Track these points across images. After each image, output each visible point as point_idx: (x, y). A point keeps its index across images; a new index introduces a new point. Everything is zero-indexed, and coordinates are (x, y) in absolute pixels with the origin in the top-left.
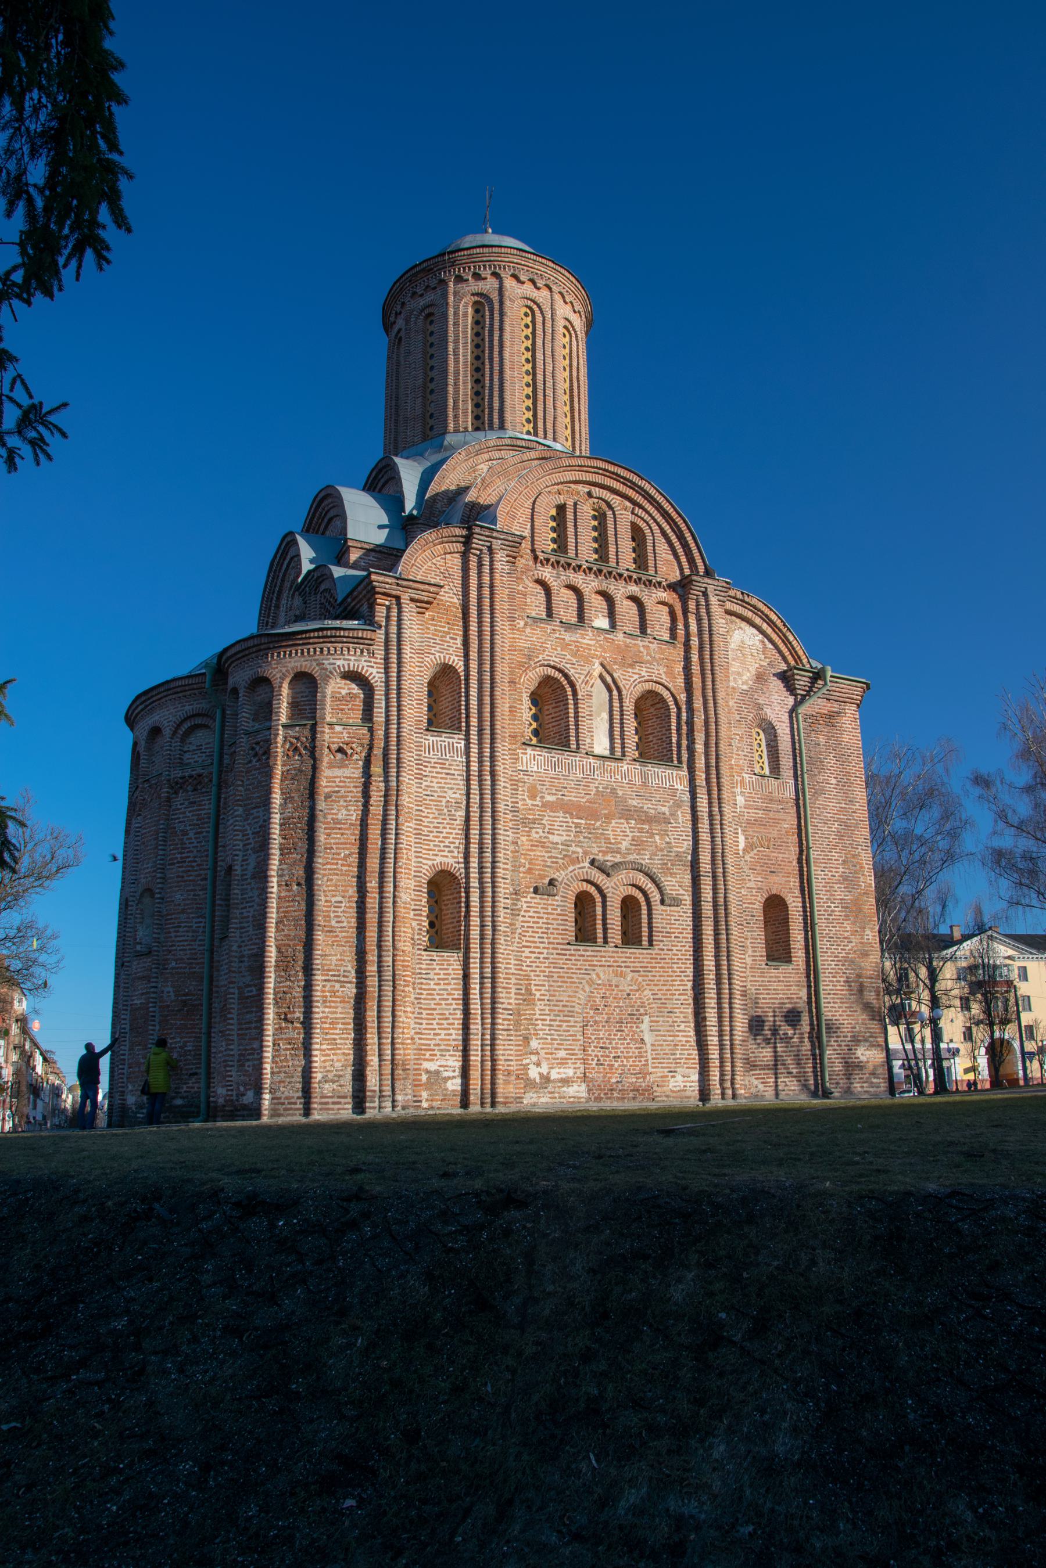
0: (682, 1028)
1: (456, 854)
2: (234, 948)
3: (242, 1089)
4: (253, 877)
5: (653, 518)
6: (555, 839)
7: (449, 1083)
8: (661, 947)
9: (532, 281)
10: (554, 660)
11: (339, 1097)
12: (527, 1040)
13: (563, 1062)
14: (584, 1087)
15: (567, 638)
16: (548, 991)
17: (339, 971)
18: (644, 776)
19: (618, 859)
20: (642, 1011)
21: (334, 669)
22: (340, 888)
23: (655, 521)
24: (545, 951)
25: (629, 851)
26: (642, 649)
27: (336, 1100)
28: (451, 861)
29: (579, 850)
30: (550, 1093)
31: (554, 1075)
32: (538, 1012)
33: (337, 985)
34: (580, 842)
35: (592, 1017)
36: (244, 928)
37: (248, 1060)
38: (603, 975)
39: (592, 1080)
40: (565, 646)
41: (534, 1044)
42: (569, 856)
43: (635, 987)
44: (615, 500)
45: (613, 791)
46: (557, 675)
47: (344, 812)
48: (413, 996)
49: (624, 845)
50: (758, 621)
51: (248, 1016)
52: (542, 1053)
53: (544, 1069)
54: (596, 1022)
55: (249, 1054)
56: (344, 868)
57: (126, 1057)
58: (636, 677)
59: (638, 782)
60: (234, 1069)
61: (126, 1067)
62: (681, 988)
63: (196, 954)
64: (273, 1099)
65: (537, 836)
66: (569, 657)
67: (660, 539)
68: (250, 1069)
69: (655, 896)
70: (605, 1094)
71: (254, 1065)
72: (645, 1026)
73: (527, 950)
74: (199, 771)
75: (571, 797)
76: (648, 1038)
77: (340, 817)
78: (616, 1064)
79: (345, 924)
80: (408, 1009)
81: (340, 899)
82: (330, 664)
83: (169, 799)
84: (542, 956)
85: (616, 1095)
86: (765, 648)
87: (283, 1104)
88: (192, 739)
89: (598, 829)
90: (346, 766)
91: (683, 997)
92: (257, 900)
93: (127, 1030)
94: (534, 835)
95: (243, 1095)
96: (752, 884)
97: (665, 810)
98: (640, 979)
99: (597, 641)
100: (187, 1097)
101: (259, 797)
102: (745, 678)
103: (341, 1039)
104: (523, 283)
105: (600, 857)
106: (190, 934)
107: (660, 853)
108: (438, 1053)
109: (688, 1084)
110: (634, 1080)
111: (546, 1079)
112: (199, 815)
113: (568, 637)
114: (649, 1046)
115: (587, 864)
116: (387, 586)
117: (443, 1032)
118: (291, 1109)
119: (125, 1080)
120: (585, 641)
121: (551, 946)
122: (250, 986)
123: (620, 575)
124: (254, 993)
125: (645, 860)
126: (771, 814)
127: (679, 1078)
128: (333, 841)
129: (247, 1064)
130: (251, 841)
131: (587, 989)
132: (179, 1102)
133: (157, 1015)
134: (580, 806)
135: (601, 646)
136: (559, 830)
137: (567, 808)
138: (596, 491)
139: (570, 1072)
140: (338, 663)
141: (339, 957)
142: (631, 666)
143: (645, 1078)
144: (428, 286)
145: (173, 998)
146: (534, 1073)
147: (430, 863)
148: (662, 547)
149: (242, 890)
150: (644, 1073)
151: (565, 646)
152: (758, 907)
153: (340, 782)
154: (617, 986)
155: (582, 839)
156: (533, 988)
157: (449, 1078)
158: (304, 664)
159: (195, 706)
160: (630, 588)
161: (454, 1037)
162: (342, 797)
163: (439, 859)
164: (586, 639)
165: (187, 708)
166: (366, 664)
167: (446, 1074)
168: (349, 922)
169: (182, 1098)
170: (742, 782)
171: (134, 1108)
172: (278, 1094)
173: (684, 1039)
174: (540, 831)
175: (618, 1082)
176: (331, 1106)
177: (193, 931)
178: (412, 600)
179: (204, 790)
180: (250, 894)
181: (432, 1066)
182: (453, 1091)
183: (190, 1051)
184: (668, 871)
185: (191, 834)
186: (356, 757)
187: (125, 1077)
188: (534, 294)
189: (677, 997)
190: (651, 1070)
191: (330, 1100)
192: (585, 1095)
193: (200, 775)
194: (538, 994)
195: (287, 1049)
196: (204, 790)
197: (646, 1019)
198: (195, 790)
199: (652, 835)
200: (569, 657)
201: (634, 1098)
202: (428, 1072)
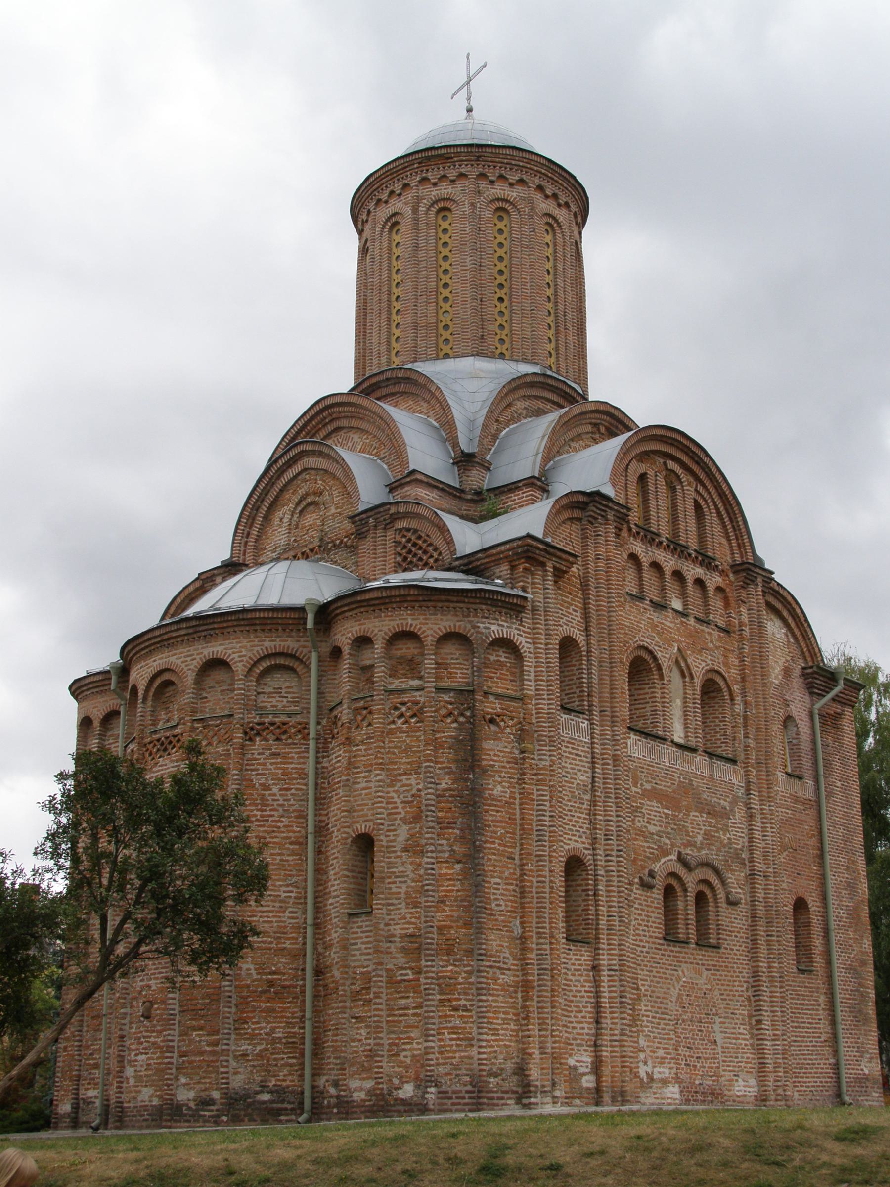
1: (584, 839)
2: (382, 926)
3: (396, 1081)
4: (405, 849)
5: (711, 496)
6: (652, 829)
7: (584, 1079)
10: (646, 642)
11: (503, 1092)
14: (676, 1089)
15: (655, 619)
16: (650, 986)
17: (499, 957)
21: (490, 633)
22: (498, 869)
23: (713, 500)
24: (647, 945)
27: (499, 1095)
29: (668, 841)
32: (644, 1008)
33: (498, 972)
34: (669, 833)
35: (681, 1015)
36: (392, 904)
37: (405, 1050)
43: (709, 987)
44: (685, 477)
47: (499, 788)
50: (785, 614)
51: (403, 1001)
52: (648, 1051)
54: (684, 1021)
55: (403, 1043)
56: (502, 848)
57: (175, 1044)
60: (385, 1059)
61: (176, 1055)
63: (286, 927)
64: (439, 1092)
65: (639, 825)
67: (716, 520)
68: (408, 1061)
69: (721, 894)
70: (693, 1096)
71: (414, 1056)
74: (284, 718)
76: (719, 1037)
77: (495, 792)
78: (698, 1065)
79: (503, 908)
81: (498, 880)
82: (485, 628)
83: (243, 747)
84: (645, 950)
86: (789, 642)
87: (451, 1098)
88: (268, 680)
90: (499, 739)
92: (412, 876)
93: (177, 1012)
95: (397, 1088)
100: (277, 1091)
101: (409, 763)
103: (502, 1029)
106: (277, 904)
107: (723, 849)
108: (576, 1048)
110: (711, 1082)
112: (283, 769)
116: (538, 552)
118: (459, 1104)
119: (174, 1071)
121: (651, 940)
122: (405, 969)
124: (411, 977)
128: (491, 818)
129: (405, 1053)
130: (400, 810)
132: (266, 1097)
133: (234, 996)
134: (667, 796)
138: (671, 464)
140: (493, 627)
141: (498, 942)
144: (444, 176)
145: (255, 977)
147: (566, 847)
148: (717, 529)
149: (389, 863)
152: (790, 908)
153: (495, 755)
157: (584, 1074)
158: (458, 624)
159: (277, 644)
161: (586, 1031)
162: (497, 771)
163: (573, 845)
165: (267, 644)
166: (517, 632)
168: (506, 906)
169: (271, 1092)
171: (192, 1105)
172: (444, 1088)
173: (743, 1042)
175: (700, 1084)
176: (496, 1102)
177: (281, 901)
179: (290, 741)
180: (401, 869)
182: (588, 1088)
183: (280, 1038)
185: (275, 790)
186: (508, 730)
187: (174, 1067)
188: (556, 212)
190: (722, 1073)
191: (495, 1095)
193: (284, 724)
195: (451, 1039)
196: (290, 741)
198: (278, 739)
200: (657, 639)
201: (712, 1102)
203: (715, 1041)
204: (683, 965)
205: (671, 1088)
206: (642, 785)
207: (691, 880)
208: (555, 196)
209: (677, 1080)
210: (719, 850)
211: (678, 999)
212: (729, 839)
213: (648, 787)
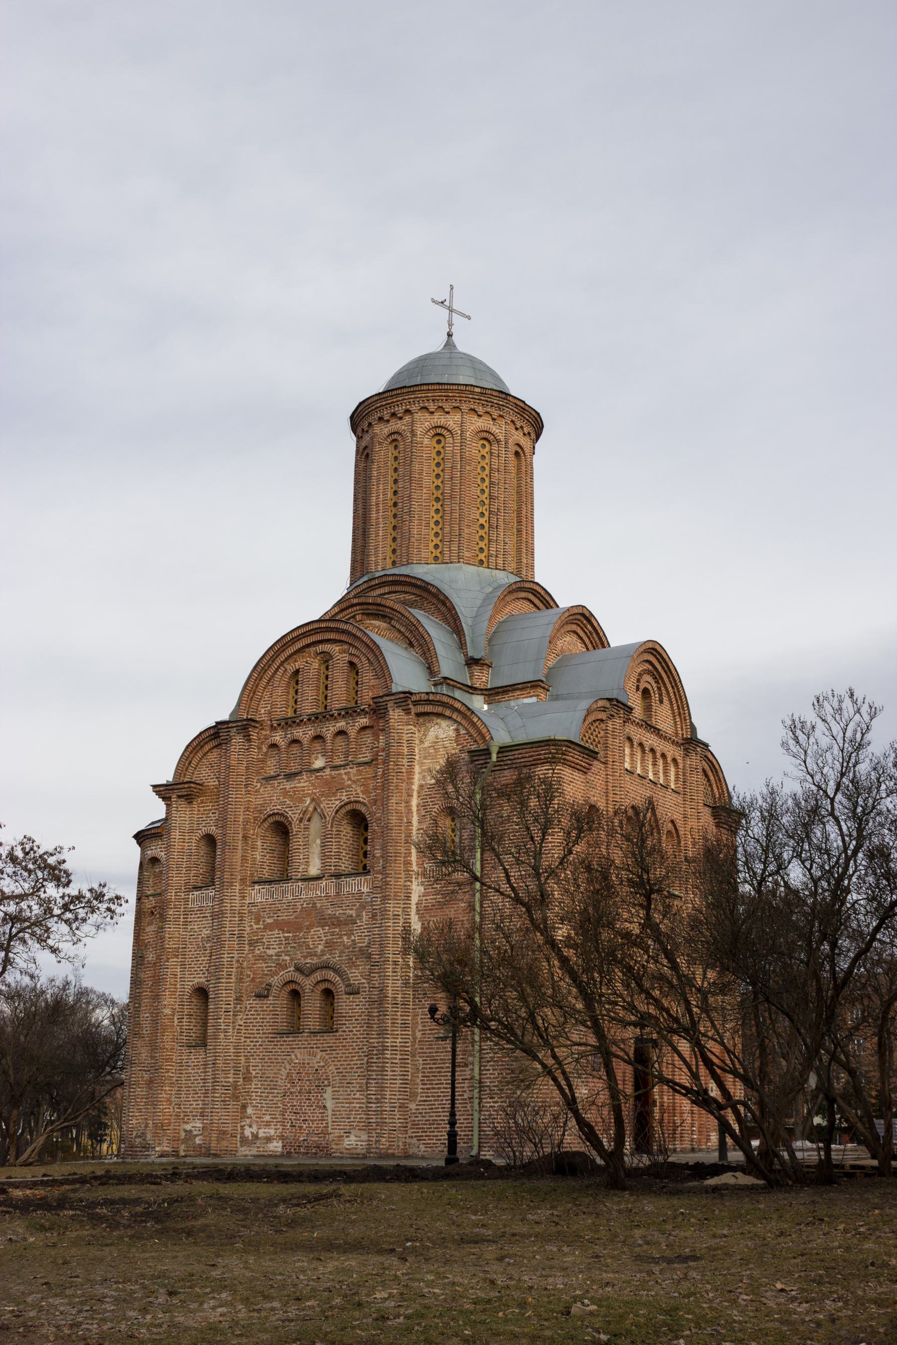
0: (357, 1096)
6: (270, 952)
7: (197, 1138)
8: (344, 1029)
9: (394, 415)
12: (244, 1107)
13: (268, 1124)
14: (280, 1144)
15: (288, 787)
18: (338, 887)
19: (315, 960)
20: (326, 1082)
25: (323, 953)
26: (344, 776)
28: (203, 980)
29: (287, 958)
30: (258, 1147)
31: (261, 1134)
39: (287, 1138)
40: (285, 793)
41: (250, 1111)
42: (279, 964)
43: (322, 1064)
46: (282, 819)
48: (174, 1079)
49: (321, 947)
50: (448, 713)
52: (254, 1117)
53: (254, 1129)
54: (291, 1093)
58: (337, 802)
59: (332, 893)
62: (359, 1062)
65: (258, 952)
66: (288, 802)
69: (342, 988)
72: (328, 1093)
75: (284, 917)
76: (329, 1104)
80: (167, 1088)
85: (302, 1150)
89: (301, 938)
91: (359, 1070)
97: (353, 913)
98: (327, 1057)
99: (310, 781)
104: (388, 421)
107: (347, 951)
109: (359, 1143)
111: (255, 1136)
113: (288, 786)
114: (330, 1112)
115: (292, 969)
117: (195, 1103)
123: (332, 716)
125: (335, 958)
127: (353, 1138)
131: (288, 1067)
134: (290, 922)
135: (313, 785)
136: (274, 944)
137: (279, 925)
138: (320, 648)
139: (272, 1132)
142: (334, 794)
143: (325, 1137)
146: (248, 1132)
147: (191, 984)
150: (325, 1133)
154: (308, 1064)
155: (289, 949)
156: (251, 1068)
157: (197, 1135)
160: (338, 725)
163: (196, 980)
164: (303, 783)
167: (195, 1133)
174: (261, 948)
178: (179, 797)
181: (188, 1127)
184: (353, 965)
189: (355, 1070)
192: (280, 1149)
194: (254, 1073)
199: (341, 937)
200: (288, 802)
202: (185, 1131)
203: (325, 1106)
204: (296, 1051)
205: (275, 1144)
206: (264, 921)
207: (307, 983)
209: (282, 1138)
210: (342, 952)
211: (287, 1076)
212: (353, 941)
213: (270, 921)
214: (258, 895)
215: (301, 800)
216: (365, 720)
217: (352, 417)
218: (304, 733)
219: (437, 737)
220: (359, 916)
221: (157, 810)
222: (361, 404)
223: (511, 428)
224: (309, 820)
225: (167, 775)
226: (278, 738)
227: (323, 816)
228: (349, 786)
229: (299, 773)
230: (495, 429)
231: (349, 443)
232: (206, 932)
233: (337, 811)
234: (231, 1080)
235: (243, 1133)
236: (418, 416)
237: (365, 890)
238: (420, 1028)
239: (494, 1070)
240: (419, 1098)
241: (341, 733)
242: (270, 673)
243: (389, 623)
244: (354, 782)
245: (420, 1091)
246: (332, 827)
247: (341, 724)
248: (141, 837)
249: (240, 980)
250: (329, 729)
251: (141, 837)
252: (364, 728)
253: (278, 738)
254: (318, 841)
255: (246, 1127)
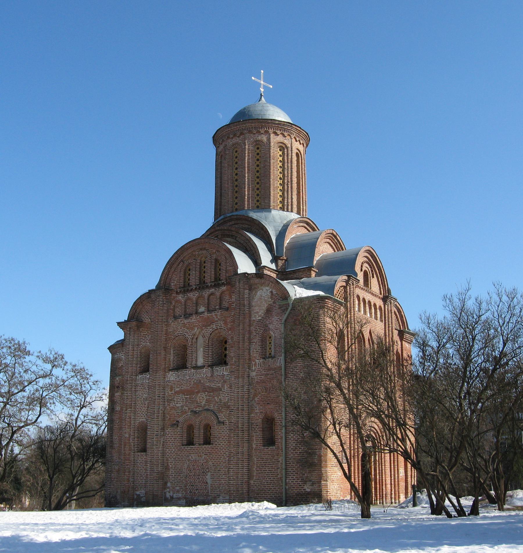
0: (223, 477)
6: (178, 405)
12: (166, 483)
13: (178, 491)
14: (185, 501)
18: (212, 372)
28: (144, 419)
29: (187, 408)
31: (175, 496)
38: (193, 457)
40: (184, 325)
41: (169, 484)
43: (205, 461)
45: (200, 381)
49: (204, 402)
53: (171, 494)
58: (211, 330)
72: (209, 476)
73: (167, 449)
76: (209, 481)
94: (171, 405)
96: (257, 411)
97: (220, 385)
98: (208, 458)
102: (260, 313)
105: (194, 410)
120: (193, 321)
126: (268, 377)
136: (179, 402)
137: (183, 392)
139: (180, 495)
142: (209, 325)
151: (184, 325)
157: (142, 497)
160: (210, 290)
163: (141, 420)
167: (141, 495)
170: (255, 364)
181: (138, 493)
190: (210, 494)
194: (171, 466)
197: (209, 474)
202: (136, 494)
205: (182, 501)
208: (235, 135)
214: (172, 376)
215: (193, 329)
216: (224, 288)
217: (213, 137)
218: (193, 295)
219: (261, 296)
220: (223, 386)
221: (120, 335)
222: (218, 130)
223: (294, 140)
224: (197, 339)
225: (124, 317)
226: (180, 298)
227: (204, 337)
228: (217, 321)
229: (191, 314)
230: (286, 142)
231: (211, 152)
232: (145, 396)
233: (211, 334)
234: (160, 469)
235: (165, 496)
236: (247, 135)
237: (226, 373)
238: (255, 442)
239: (293, 463)
240: (255, 478)
241: (212, 294)
242: (175, 266)
243: (235, 239)
244: (219, 319)
245: (255, 474)
246: (208, 342)
247: (213, 290)
248: (111, 348)
249: (164, 420)
250: (206, 293)
251: (111, 348)
252: (223, 292)
253: (180, 298)
254: (202, 349)
255: (167, 493)
